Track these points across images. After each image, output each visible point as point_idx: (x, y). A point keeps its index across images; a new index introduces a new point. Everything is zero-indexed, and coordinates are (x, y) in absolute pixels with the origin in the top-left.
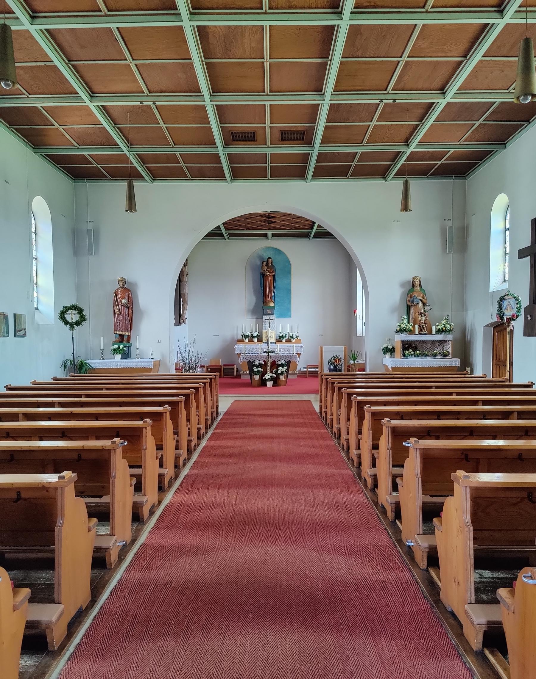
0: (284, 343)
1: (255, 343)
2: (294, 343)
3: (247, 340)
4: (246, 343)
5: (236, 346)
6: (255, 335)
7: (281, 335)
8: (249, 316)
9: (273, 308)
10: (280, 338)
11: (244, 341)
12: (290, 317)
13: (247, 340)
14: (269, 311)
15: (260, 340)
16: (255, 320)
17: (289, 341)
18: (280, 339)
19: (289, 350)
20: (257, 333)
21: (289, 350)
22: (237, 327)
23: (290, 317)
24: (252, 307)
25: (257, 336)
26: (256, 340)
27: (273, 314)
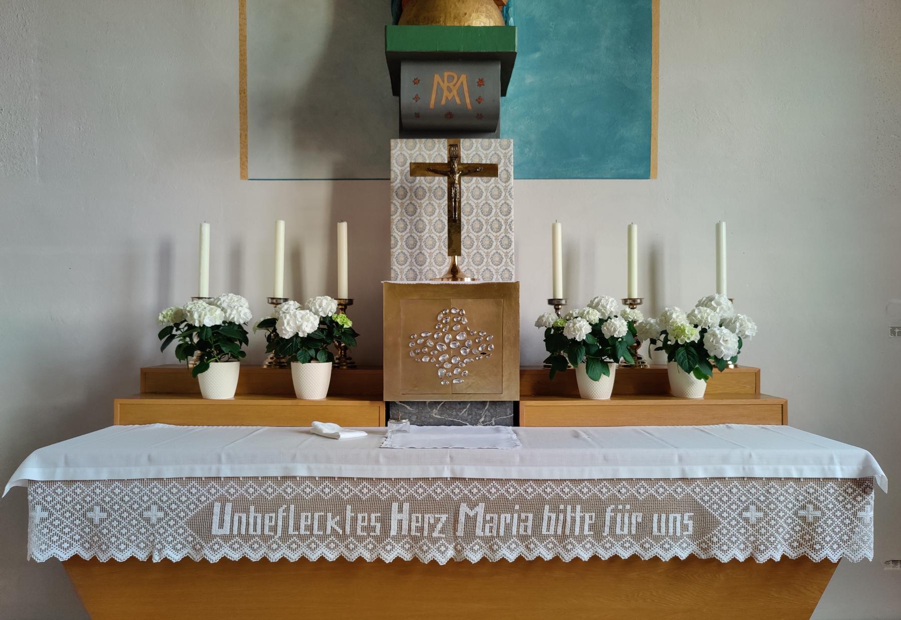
0: (604, 418)
1: (306, 417)
2: (704, 415)
3: (222, 380)
4: (221, 415)
5: (32, 470)
6: (300, 322)
7: (581, 330)
8: (274, 157)
9: (495, 58)
10: (556, 363)
11: (194, 391)
12: (639, 164)
13: (222, 380)
14: (448, 88)
15: (361, 375)
16: (320, 193)
17: (646, 385)
18: (558, 369)
19: (705, 525)
20: (329, 306)
21: (705, 525)
22: (166, 255)
23: (639, 164)
24: (293, 72)
25: (325, 341)
26: (314, 378)
27: (484, 125)
